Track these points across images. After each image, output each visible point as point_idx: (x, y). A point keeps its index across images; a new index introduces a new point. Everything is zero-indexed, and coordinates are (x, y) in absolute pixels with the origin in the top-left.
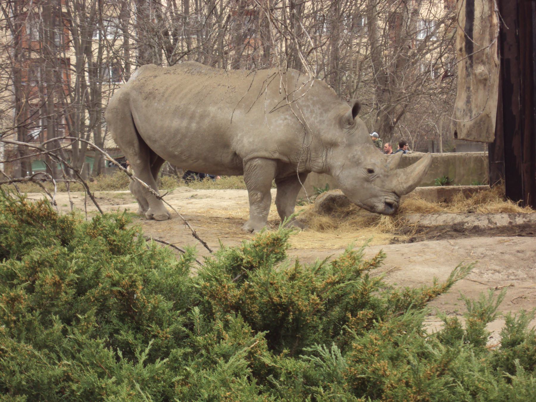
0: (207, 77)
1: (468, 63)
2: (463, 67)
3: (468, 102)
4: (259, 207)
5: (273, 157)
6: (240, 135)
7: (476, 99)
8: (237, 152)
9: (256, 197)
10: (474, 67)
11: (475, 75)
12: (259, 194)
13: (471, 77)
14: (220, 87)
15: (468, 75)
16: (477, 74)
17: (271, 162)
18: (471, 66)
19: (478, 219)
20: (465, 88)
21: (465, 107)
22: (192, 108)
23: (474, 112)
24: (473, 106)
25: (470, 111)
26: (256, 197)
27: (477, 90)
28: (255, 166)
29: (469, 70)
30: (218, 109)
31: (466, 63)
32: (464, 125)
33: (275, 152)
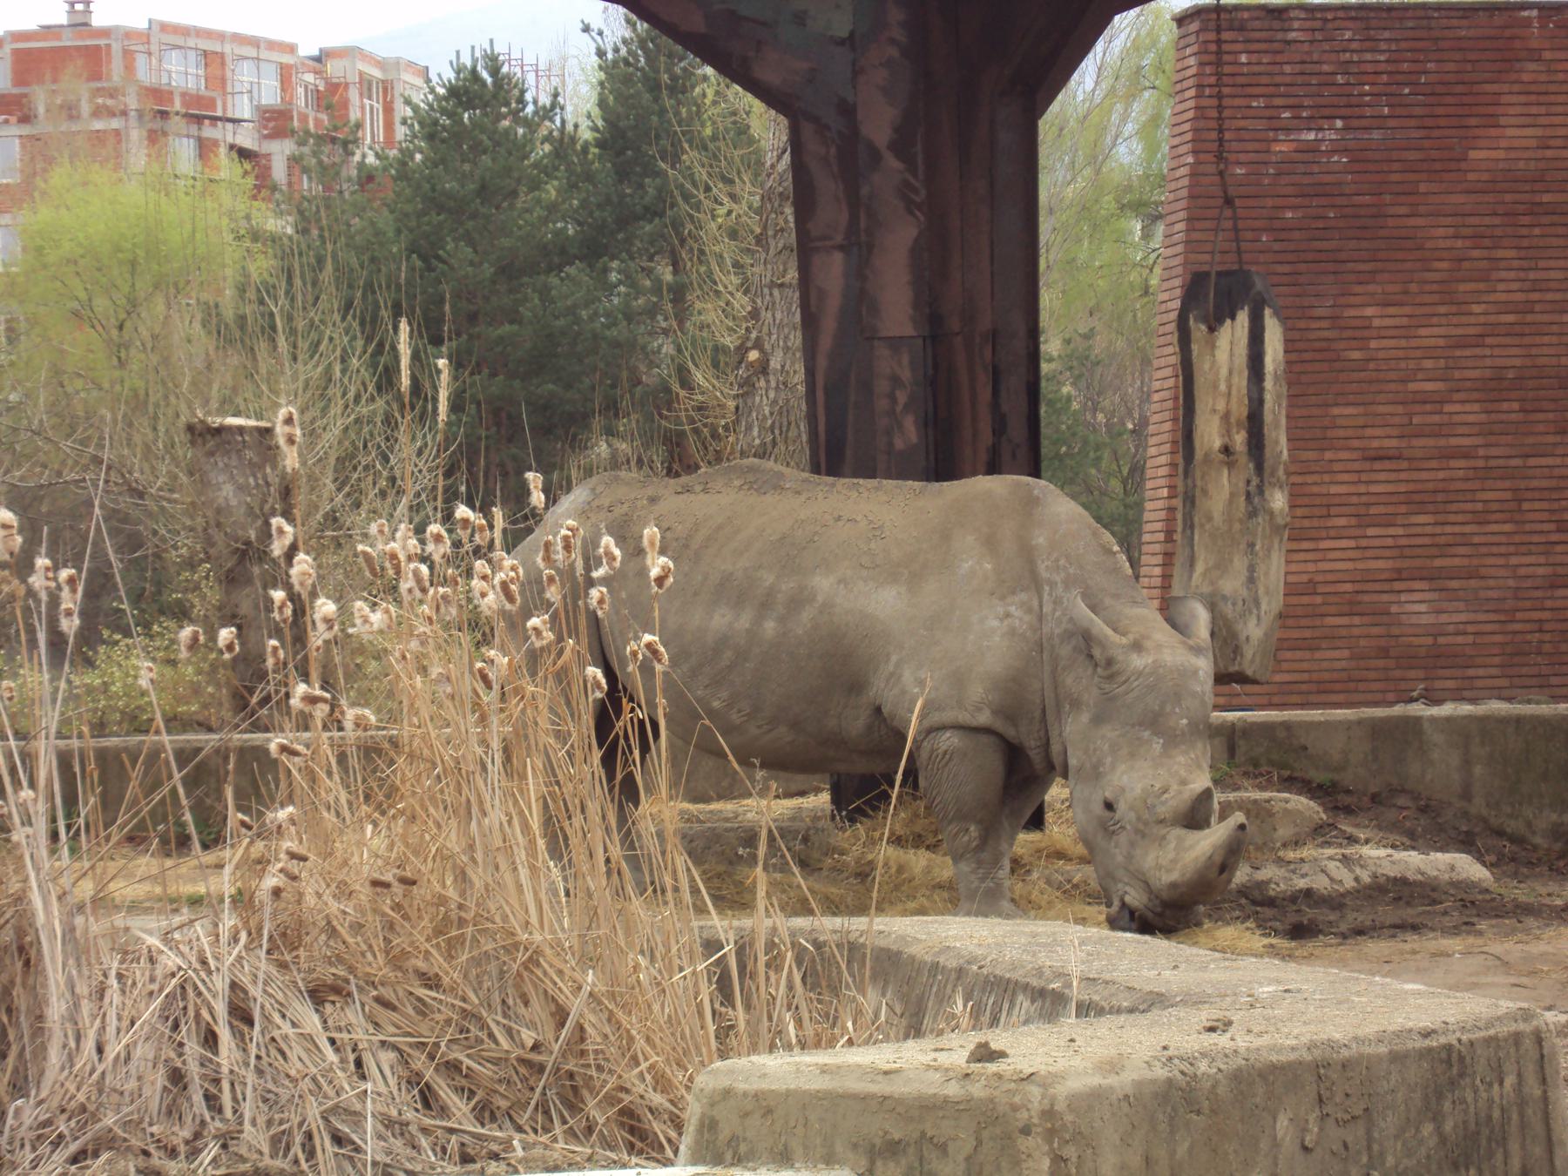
0: (803, 498)
1: (1254, 483)
2: (1232, 495)
3: (1251, 580)
4: (980, 863)
5: (975, 723)
6: (894, 658)
7: (1267, 574)
8: (885, 711)
9: (966, 838)
10: (1267, 494)
11: (1271, 513)
12: (972, 828)
13: (1260, 520)
14: (840, 524)
15: (1252, 514)
16: (1277, 512)
17: (985, 739)
18: (1261, 490)
19: (1294, 872)
20: (1243, 546)
21: (1245, 593)
22: (768, 578)
23: (1264, 607)
24: (1261, 591)
25: (1257, 603)
26: (966, 838)
27: (1269, 550)
28: (945, 752)
29: (1256, 500)
30: (839, 582)
31: (1248, 482)
32: (1248, 638)
33: (979, 709)
